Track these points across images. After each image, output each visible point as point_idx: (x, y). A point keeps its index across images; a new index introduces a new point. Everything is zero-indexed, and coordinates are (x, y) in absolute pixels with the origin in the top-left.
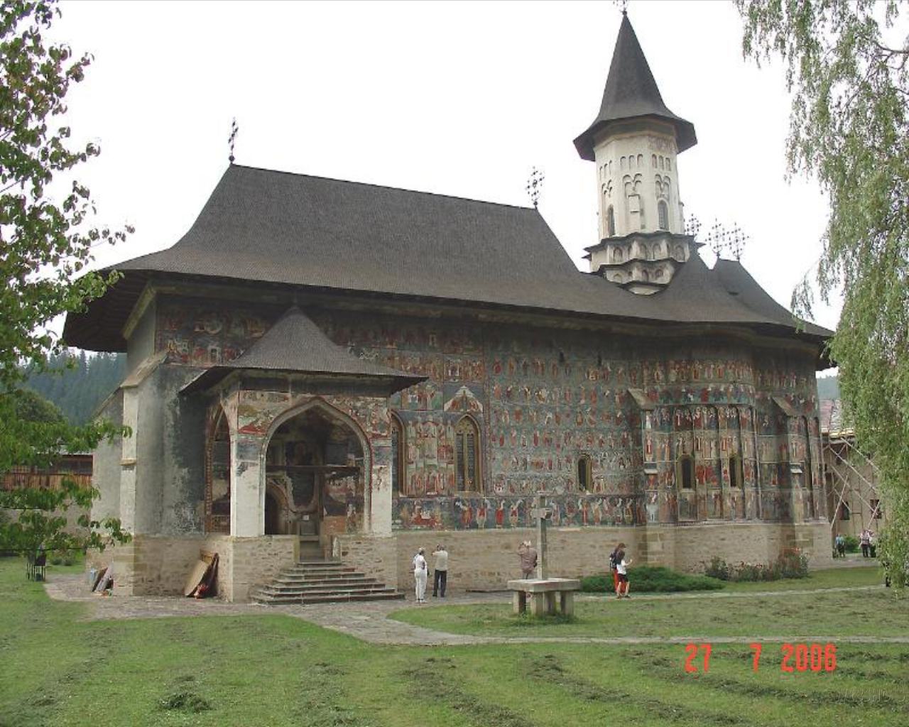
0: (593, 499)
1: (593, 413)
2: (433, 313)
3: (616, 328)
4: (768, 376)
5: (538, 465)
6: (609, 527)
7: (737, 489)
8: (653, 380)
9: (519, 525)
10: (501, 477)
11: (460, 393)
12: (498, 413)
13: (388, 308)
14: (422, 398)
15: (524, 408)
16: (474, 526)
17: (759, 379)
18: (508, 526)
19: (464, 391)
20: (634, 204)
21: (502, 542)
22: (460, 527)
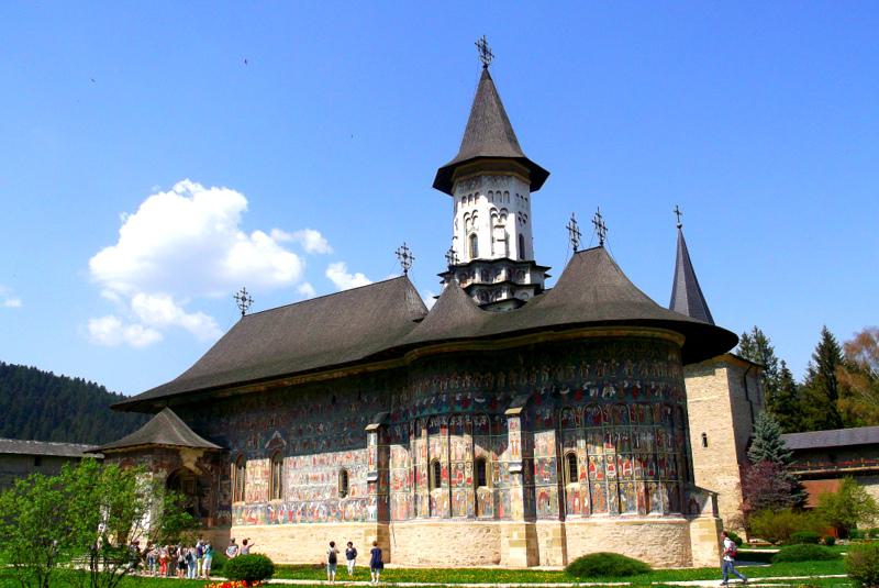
0: (349, 502)
1: (352, 436)
2: (262, 388)
3: (371, 368)
4: (513, 375)
5: (315, 478)
6: (358, 523)
7: (439, 490)
8: (399, 402)
9: (302, 521)
10: (293, 489)
11: (273, 437)
12: (294, 446)
13: (241, 391)
14: (255, 442)
15: (309, 440)
16: (277, 522)
17: (503, 380)
18: (295, 522)
19: (277, 434)
20: (499, 234)
21: (289, 533)
22: (270, 523)
